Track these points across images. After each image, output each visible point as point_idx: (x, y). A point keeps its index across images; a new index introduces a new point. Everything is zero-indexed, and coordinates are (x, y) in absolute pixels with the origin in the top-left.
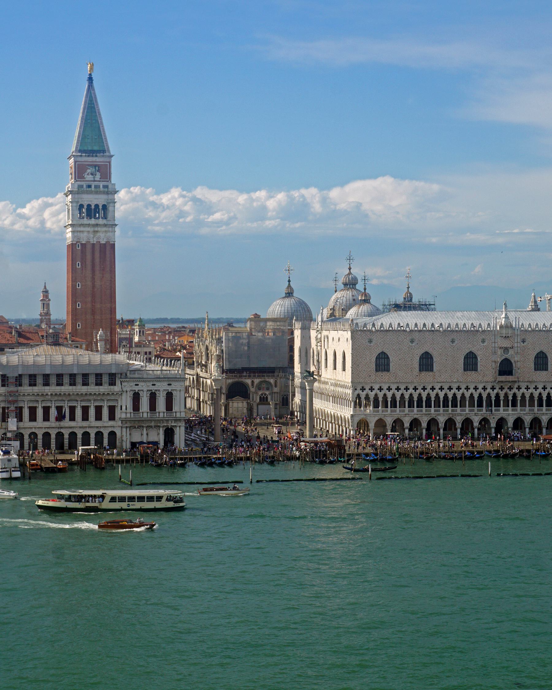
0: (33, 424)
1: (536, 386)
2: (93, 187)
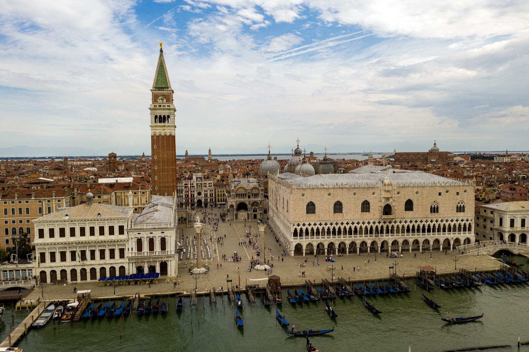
0: (63, 263)
1: (406, 221)
2: (162, 106)
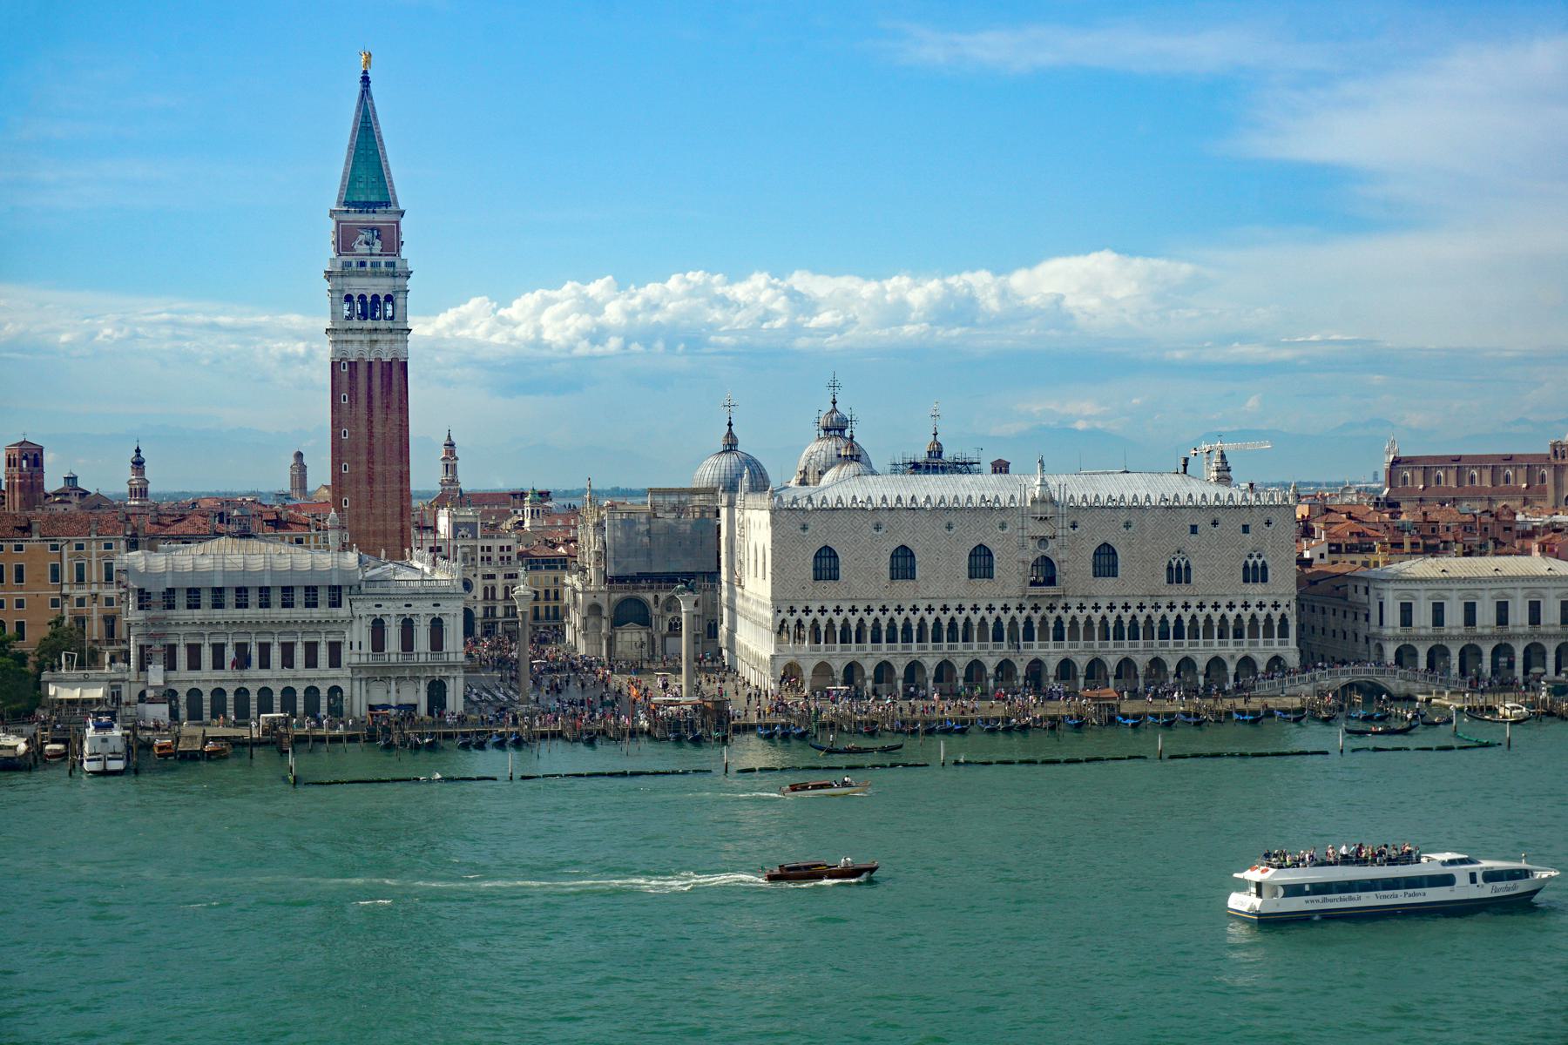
1: (1096, 604)
2: (368, 264)
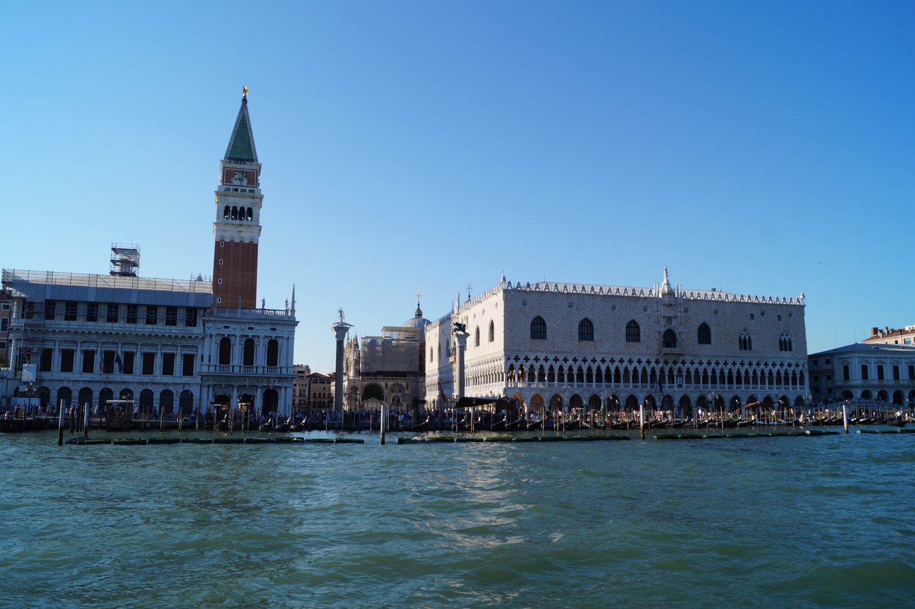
2: (239, 190)
